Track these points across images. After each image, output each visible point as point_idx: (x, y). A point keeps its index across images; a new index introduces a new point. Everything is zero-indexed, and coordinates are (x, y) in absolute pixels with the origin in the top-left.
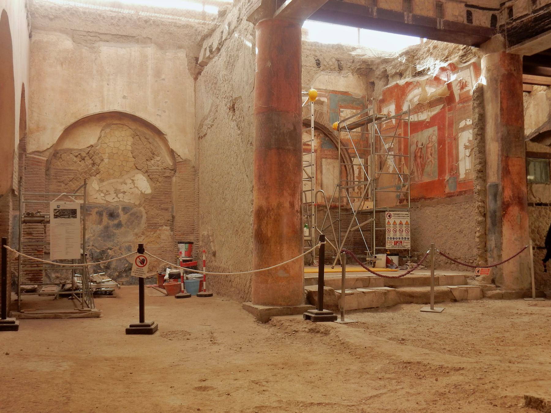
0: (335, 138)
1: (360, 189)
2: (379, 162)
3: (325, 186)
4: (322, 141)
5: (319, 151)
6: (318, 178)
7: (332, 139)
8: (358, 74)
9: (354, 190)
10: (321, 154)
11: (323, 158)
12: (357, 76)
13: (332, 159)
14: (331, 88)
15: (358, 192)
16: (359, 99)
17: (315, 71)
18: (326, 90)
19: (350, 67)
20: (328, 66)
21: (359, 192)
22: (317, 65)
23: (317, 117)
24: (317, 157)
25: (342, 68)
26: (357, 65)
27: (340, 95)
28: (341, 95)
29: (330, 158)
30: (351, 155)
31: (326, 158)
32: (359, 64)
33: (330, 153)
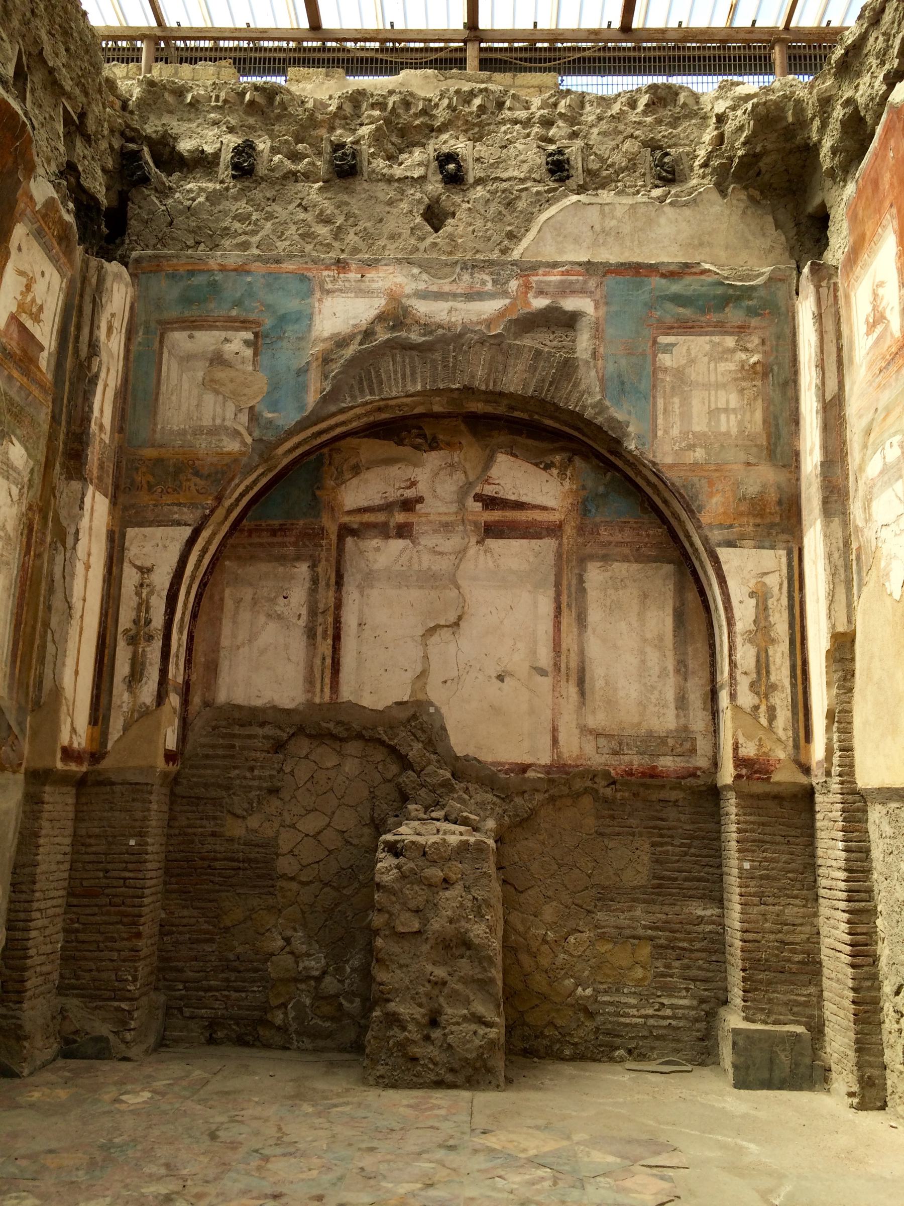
0: (641, 468)
1: (766, 697)
2: (854, 557)
3: (600, 683)
4: (584, 488)
5: (569, 530)
6: (564, 646)
7: (631, 473)
8: (745, 188)
9: (733, 696)
10: (580, 540)
11: (592, 557)
12: (743, 196)
13: (636, 561)
14: (610, 255)
15: (756, 708)
16: (752, 288)
17: (538, 193)
18: (589, 267)
19: (705, 165)
20: (605, 173)
21: (763, 708)
22: (552, 172)
23: (543, 381)
24: (559, 556)
25: (673, 172)
26: (737, 144)
27: (657, 282)
28: (663, 281)
29: (625, 559)
30: (716, 536)
31: (605, 558)
32: (742, 139)
33: (627, 535)
